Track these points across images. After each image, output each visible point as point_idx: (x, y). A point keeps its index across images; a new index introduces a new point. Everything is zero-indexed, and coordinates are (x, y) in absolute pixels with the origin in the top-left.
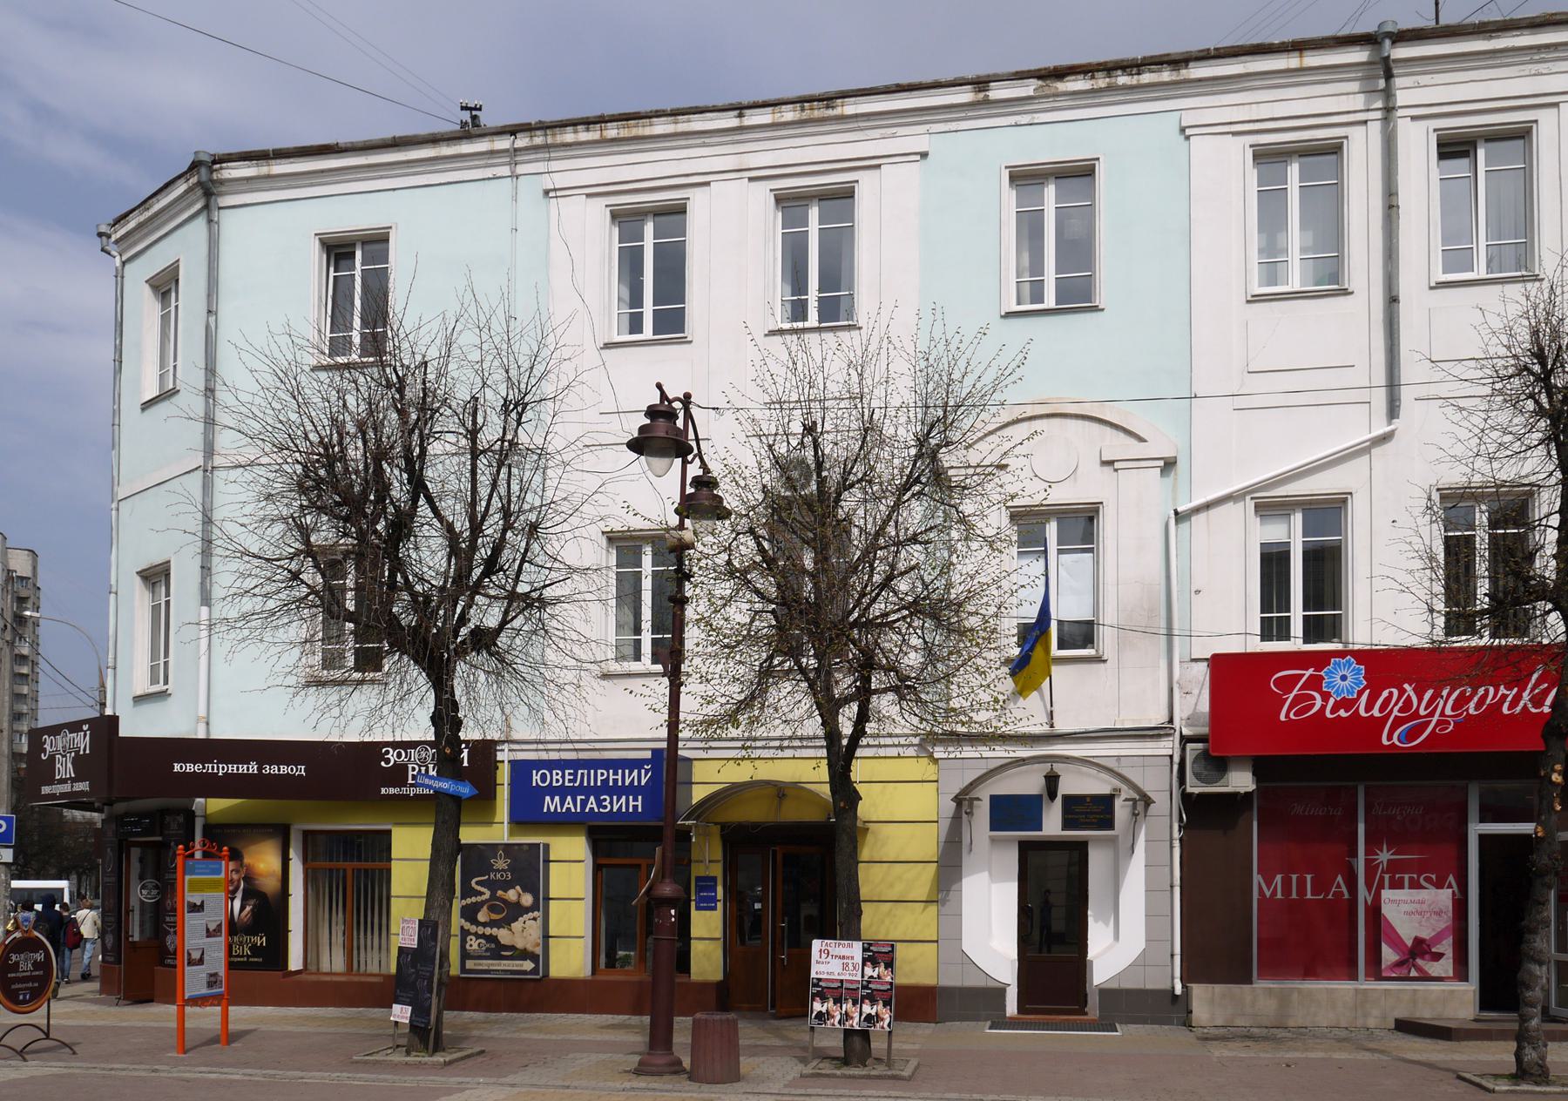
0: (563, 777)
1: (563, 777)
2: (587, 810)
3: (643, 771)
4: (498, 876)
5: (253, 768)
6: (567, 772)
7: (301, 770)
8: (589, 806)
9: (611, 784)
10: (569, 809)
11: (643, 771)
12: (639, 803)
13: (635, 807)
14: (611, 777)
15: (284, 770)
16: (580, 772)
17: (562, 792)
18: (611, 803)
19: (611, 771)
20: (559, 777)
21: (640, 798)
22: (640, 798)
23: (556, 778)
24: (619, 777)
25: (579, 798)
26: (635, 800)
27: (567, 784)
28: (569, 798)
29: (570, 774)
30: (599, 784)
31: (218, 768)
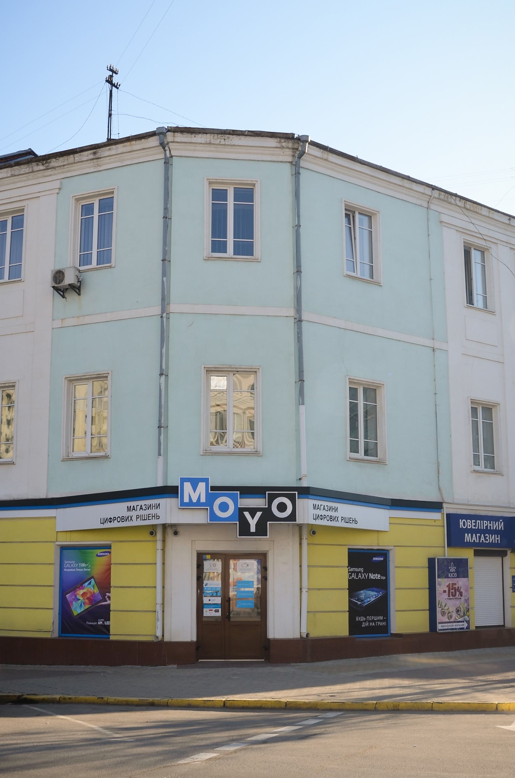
0: (471, 524)
1: (471, 524)
2: (481, 542)
3: (500, 522)
4: (452, 575)
6: (473, 521)
8: (482, 539)
9: (489, 528)
10: (474, 540)
11: (500, 522)
12: (499, 539)
13: (498, 540)
14: (489, 525)
16: (478, 521)
17: (471, 531)
18: (489, 538)
19: (489, 522)
20: (470, 524)
21: (499, 536)
22: (499, 536)
23: (469, 524)
24: (492, 525)
25: (478, 535)
26: (498, 537)
27: (473, 528)
28: (474, 535)
29: (474, 522)
30: (485, 528)
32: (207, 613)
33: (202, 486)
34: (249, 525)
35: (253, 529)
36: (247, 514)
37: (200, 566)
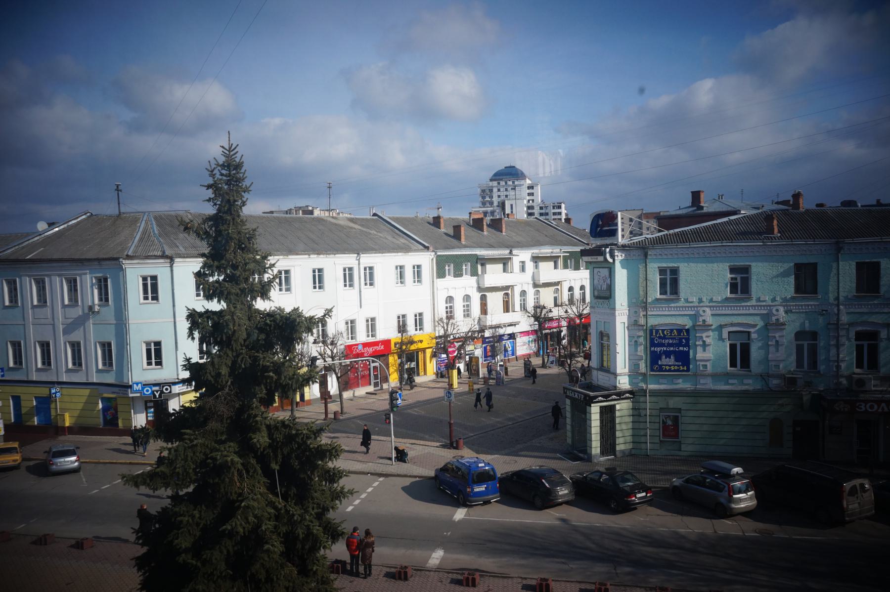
32: (149, 419)
33: (140, 385)
34: (156, 396)
35: (157, 397)
36: (155, 392)
37: (146, 405)
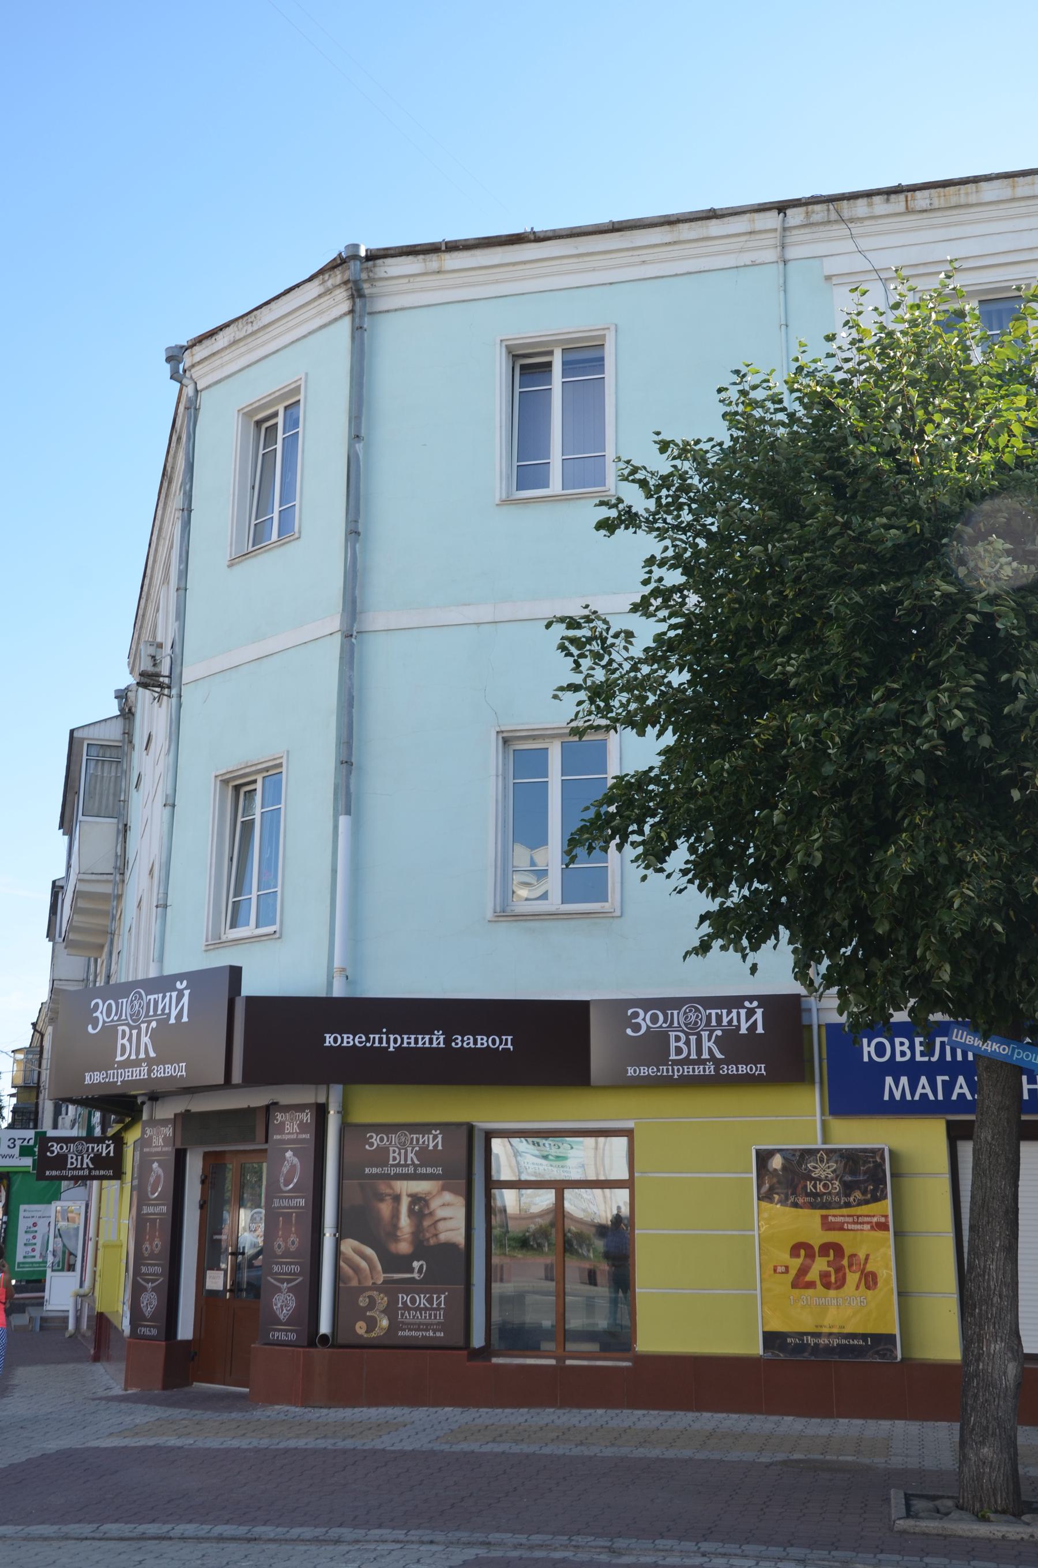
5: (438, 1040)
7: (507, 1042)
15: (483, 1042)
28: (923, 1080)
31: (388, 1040)
